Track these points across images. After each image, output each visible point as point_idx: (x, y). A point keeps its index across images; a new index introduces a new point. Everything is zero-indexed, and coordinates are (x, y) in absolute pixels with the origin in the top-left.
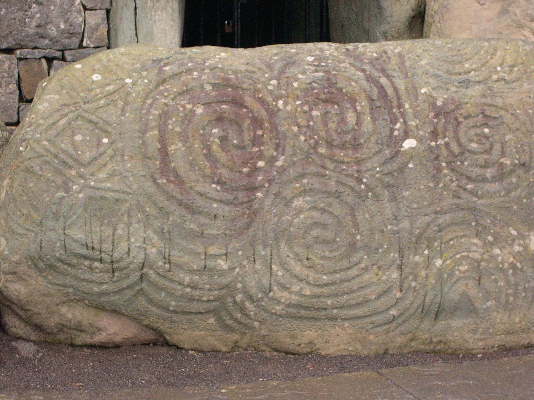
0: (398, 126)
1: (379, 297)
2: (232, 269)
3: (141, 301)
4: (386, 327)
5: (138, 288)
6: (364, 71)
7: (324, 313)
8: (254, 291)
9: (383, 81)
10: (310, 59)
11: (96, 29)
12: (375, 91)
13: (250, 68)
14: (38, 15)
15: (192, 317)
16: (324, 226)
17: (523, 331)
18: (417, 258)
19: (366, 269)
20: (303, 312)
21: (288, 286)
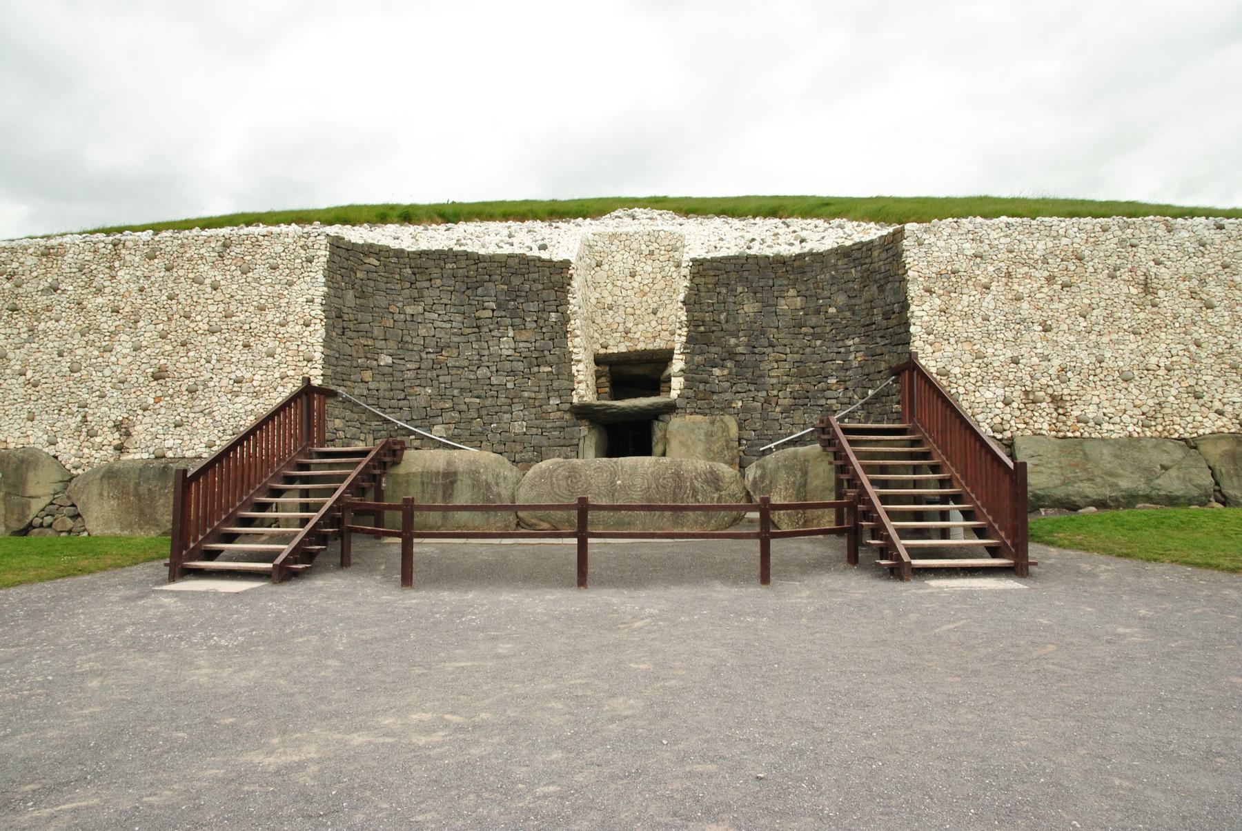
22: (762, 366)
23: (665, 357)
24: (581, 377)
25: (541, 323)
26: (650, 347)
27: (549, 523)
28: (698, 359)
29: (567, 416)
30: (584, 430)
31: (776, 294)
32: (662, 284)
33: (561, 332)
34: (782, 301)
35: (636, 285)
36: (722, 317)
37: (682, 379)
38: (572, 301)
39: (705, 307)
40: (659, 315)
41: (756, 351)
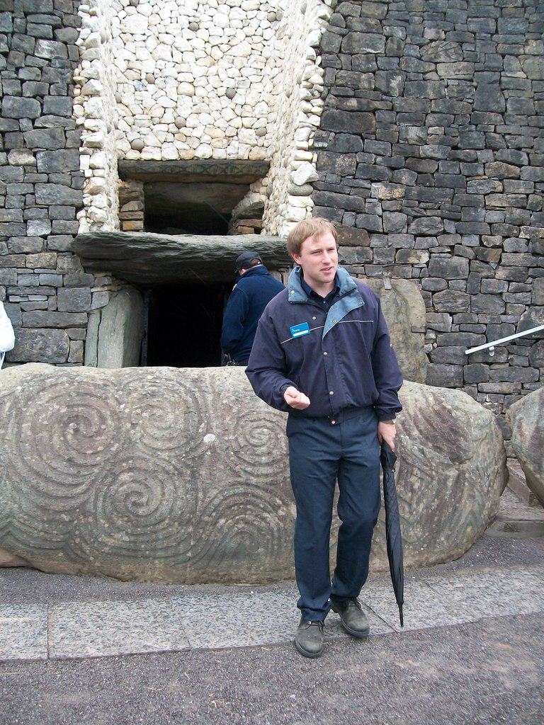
0: (203, 425)
1: (179, 544)
2: (71, 521)
3: (9, 540)
4: (184, 564)
5: (7, 530)
6: (185, 387)
7: (139, 553)
8: (87, 537)
9: (197, 394)
10: (150, 377)
11: (77, 351)
12: (190, 400)
13: (106, 382)
14: (41, 342)
15: (47, 551)
16: (139, 494)
17: (285, 569)
18: (206, 518)
19: (169, 525)
20: (124, 552)
21: (112, 534)
22: (474, 186)
23: (257, 171)
24: (97, 182)
25: (17, 58)
26: (220, 154)
27: (10, 550)
28: (342, 161)
29: (65, 263)
30: (100, 294)
31: (501, 48)
32: (244, 48)
33: (63, 80)
34: (515, 64)
35: (199, 44)
36: (394, 84)
37: (309, 201)
38: (86, 19)
39: (360, 61)
40: (238, 99)
41: (461, 154)
